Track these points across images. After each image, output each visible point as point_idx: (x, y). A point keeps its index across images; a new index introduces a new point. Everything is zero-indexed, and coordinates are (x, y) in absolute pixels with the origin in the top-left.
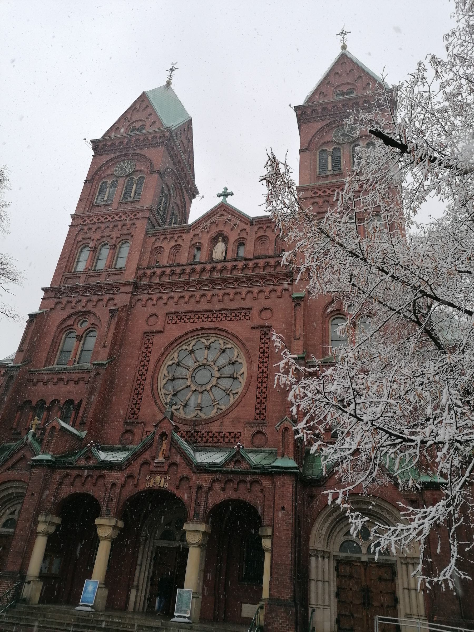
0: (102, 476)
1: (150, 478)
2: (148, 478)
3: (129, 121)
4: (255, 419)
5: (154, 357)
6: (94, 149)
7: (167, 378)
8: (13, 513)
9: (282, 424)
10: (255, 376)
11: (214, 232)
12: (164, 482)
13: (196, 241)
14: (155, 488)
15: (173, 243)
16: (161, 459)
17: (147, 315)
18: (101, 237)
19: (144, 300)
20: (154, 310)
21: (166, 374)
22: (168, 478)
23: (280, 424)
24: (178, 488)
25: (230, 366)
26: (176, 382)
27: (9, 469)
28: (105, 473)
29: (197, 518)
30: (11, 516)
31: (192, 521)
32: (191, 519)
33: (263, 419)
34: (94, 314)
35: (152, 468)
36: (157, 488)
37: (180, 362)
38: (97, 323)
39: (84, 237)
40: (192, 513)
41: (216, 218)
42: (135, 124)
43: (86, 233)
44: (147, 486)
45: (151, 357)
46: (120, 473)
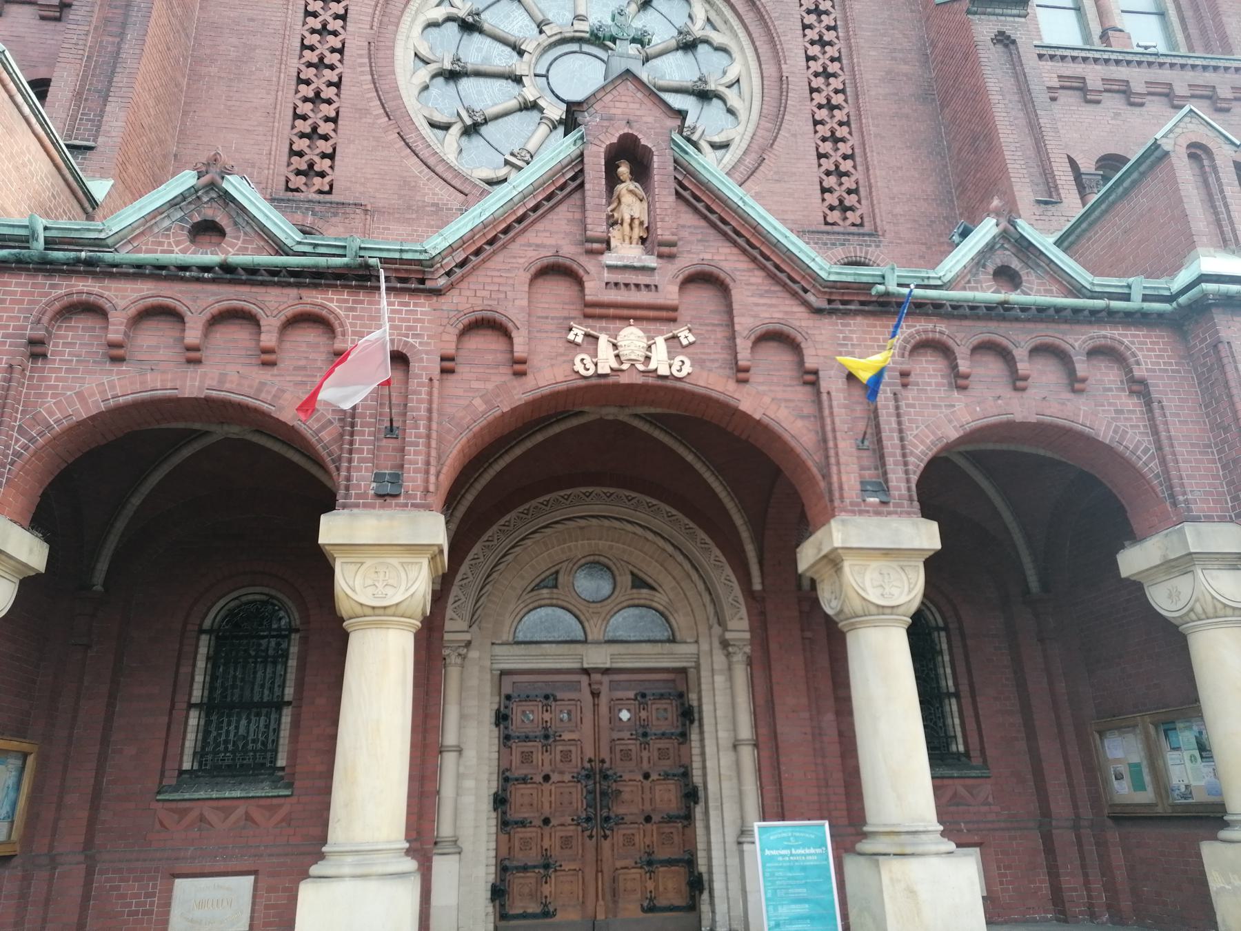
1: (587, 335)
2: (577, 334)
4: (827, 223)
7: (433, 67)
9: (1178, 130)
10: (798, 88)
12: (671, 356)
14: (624, 379)
21: (425, 52)
22: (686, 336)
23: (1171, 131)
25: (680, 54)
26: (465, 83)
28: (332, 302)
31: (859, 509)
32: (852, 504)
33: (853, 225)
35: (594, 289)
36: (639, 380)
37: (478, 14)
44: (579, 367)
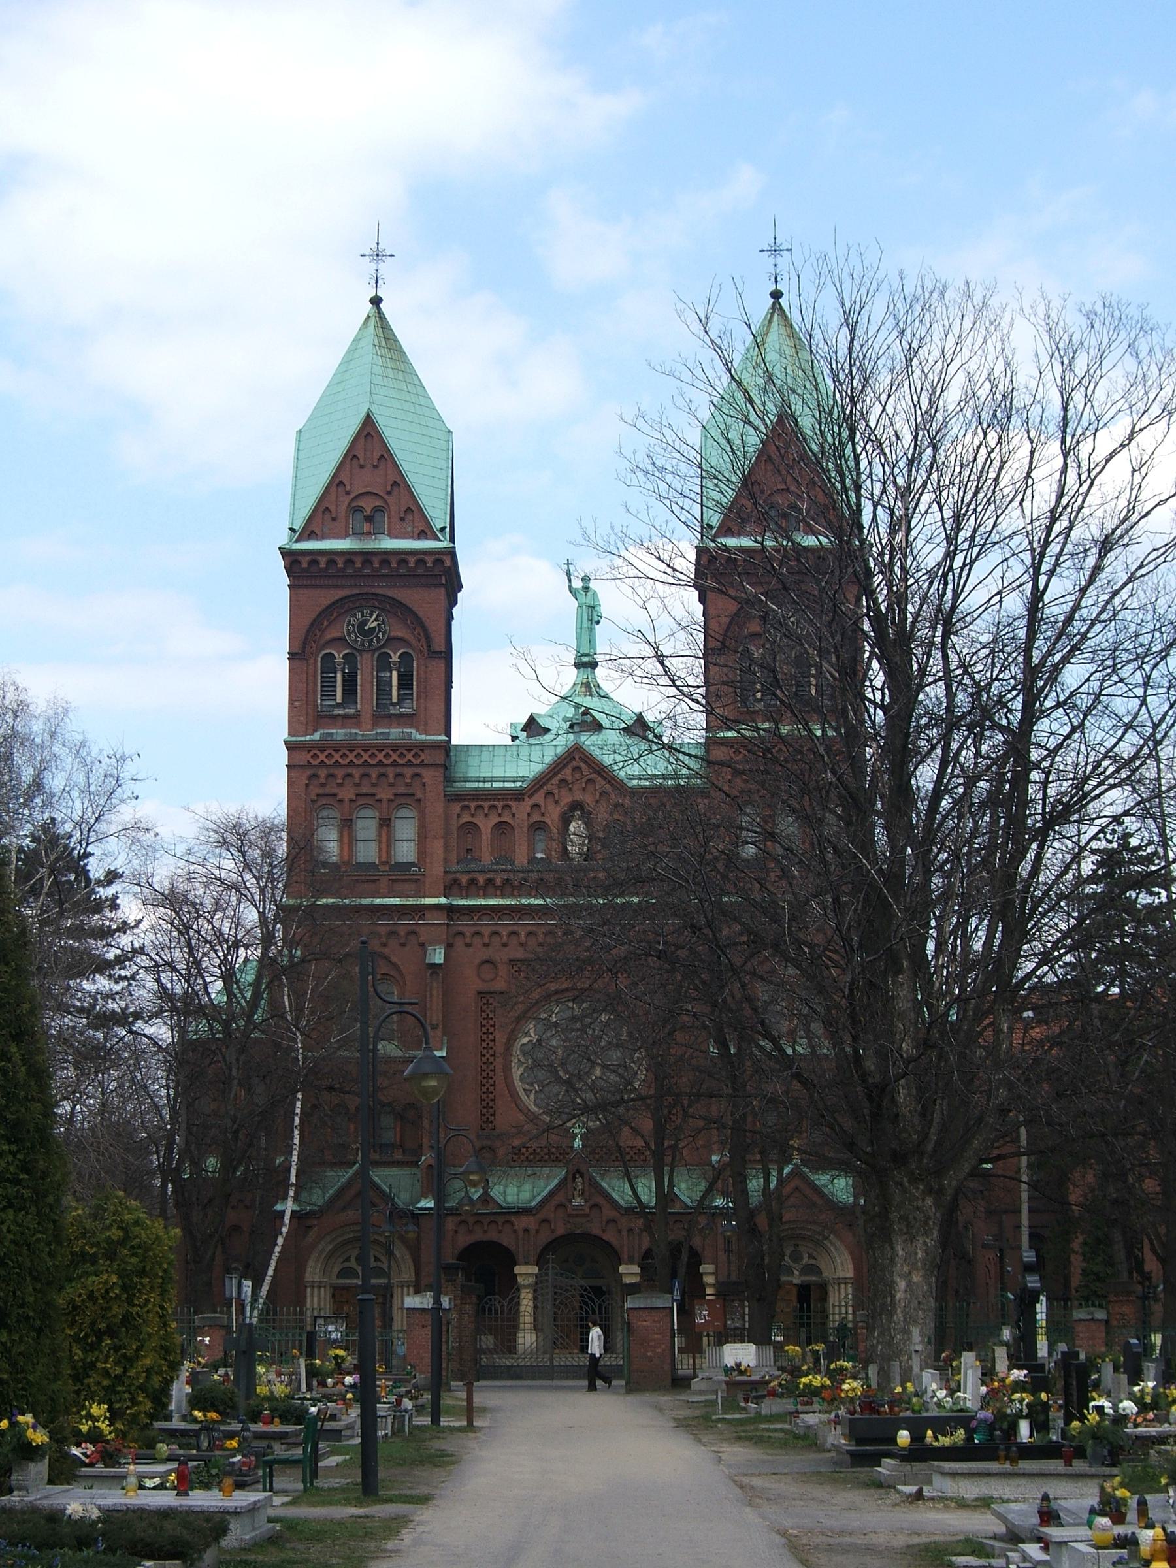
0: (511, 1223)
3: (348, 493)
5: (500, 1037)
6: (289, 570)
8: (348, 1260)
11: (567, 799)
13: (536, 817)
15: (494, 819)
16: (578, 1201)
17: (477, 961)
18: (357, 795)
19: (468, 934)
20: (484, 954)
24: (604, 1231)
27: (344, 1208)
28: (513, 1219)
29: (631, 1261)
30: (346, 1265)
34: (387, 959)
38: (392, 973)
39: (321, 791)
40: (626, 1257)
41: (567, 773)
42: (361, 502)
43: (323, 785)
45: (498, 1035)
46: (532, 1218)
